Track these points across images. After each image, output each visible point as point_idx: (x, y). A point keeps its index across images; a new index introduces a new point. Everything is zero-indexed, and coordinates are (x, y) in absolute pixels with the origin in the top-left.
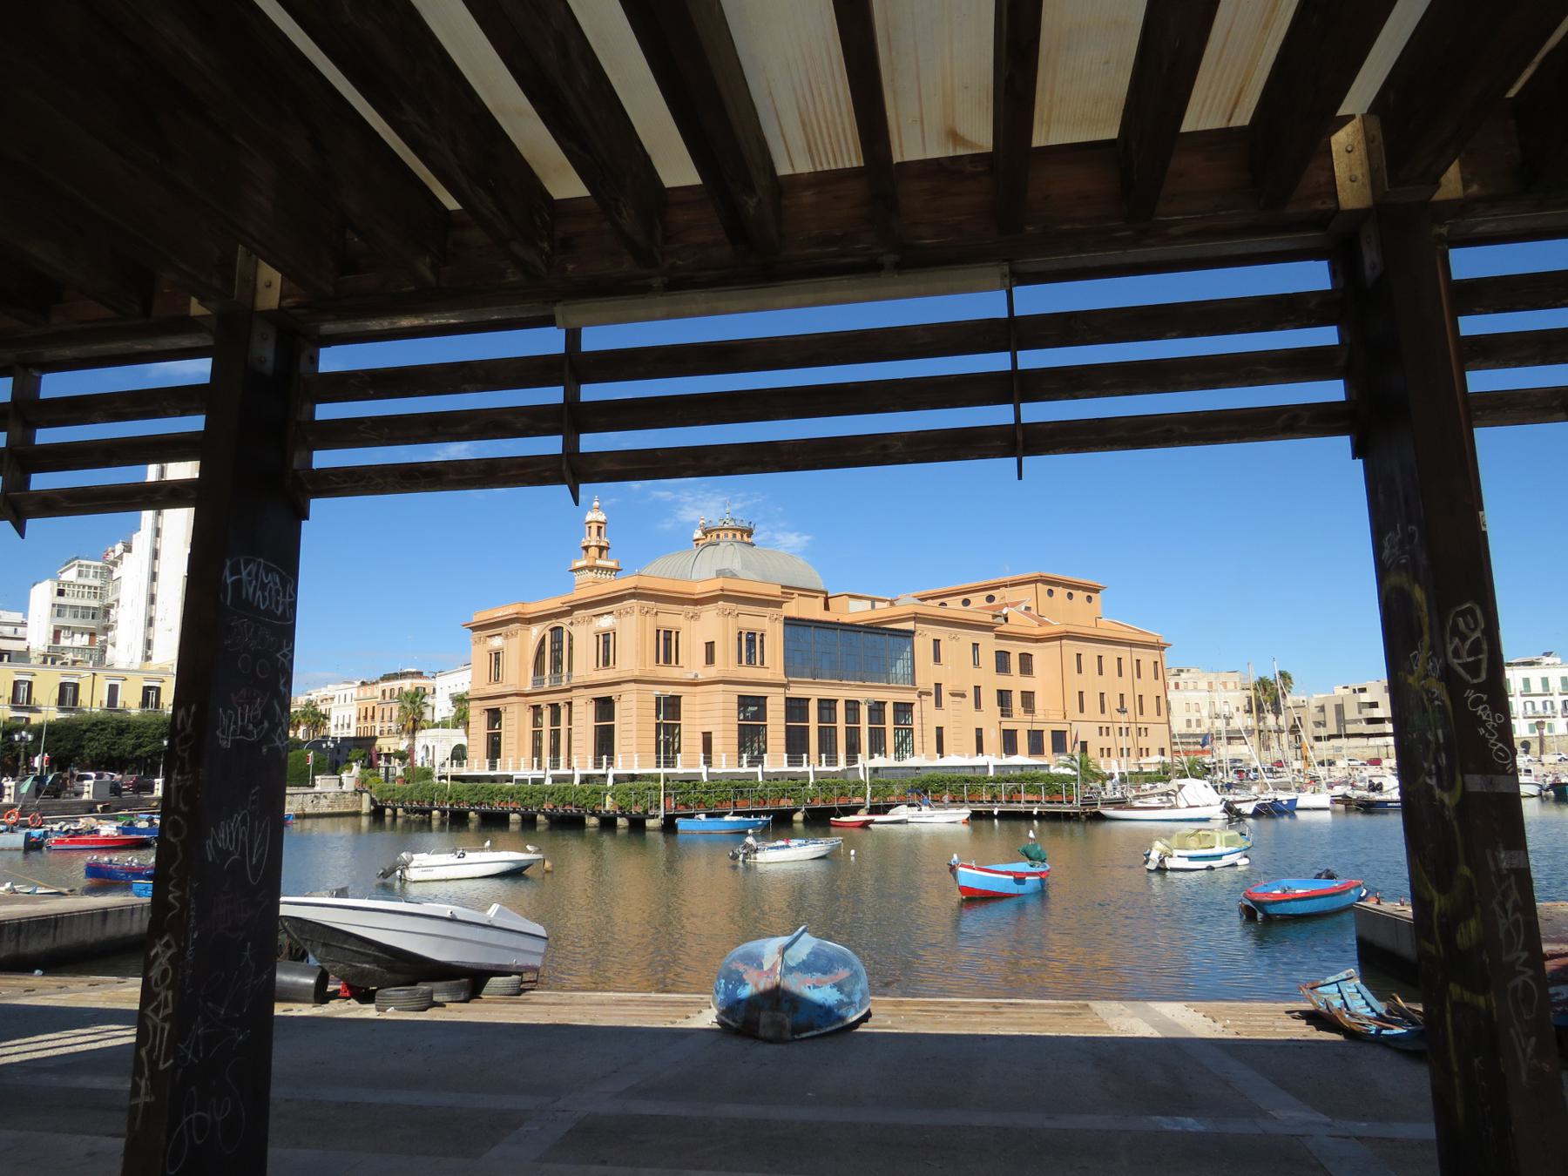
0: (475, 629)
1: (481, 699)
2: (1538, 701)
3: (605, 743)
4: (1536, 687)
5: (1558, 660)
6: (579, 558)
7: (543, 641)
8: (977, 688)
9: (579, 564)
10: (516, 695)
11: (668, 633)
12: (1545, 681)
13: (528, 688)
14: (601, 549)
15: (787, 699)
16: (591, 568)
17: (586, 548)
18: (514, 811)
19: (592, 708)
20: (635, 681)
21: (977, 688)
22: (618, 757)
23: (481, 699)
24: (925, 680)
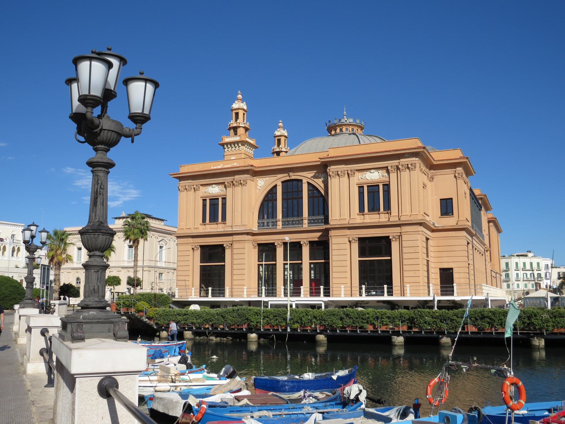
0: (181, 178)
1: (193, 237)
2: (529, 273)
4: (528, 267)
5: (532, 255)
6: (228, 135)
7: (272, 192)
9: (227, 140)
10: (248, 234)
12: (531, 264)
13: (255, 229)
14: (247, 129)
16: (244, 143)
17: (235, 129)
18: (398, 334)
19: (355, 246)
20: (420, 224)
23: (193, 237)
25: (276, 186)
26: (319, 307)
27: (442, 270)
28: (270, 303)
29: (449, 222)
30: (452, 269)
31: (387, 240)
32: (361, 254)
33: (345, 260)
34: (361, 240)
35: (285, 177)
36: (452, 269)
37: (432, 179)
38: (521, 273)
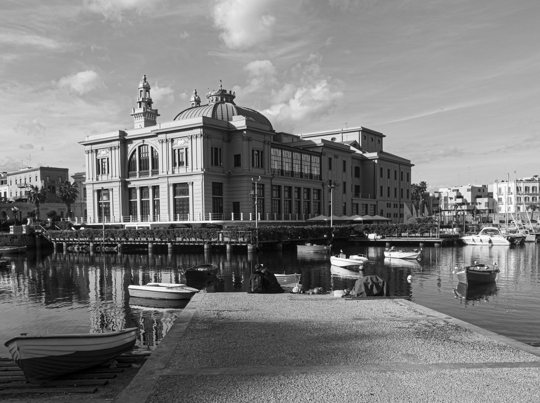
3: (181, 207)
8: (345, 183)
9: (136, 112)
11: (216, 149)
15: (272, 186)
19: (171, 188)
21: (345, 183)
22: (190, 216)
24: (325, 178)
25: (135, 150)
26: (148, 228)
27: (234, 203)
28: (126, 226)
29: (238, 169)
30: (239, 202)
31: (186, 184)
32: (175, 194)
33: (165, 198)
34: (175, 185)
35: (140, 142)
36: (239, 202)
37: (229, 141)
38: (513, 197)
